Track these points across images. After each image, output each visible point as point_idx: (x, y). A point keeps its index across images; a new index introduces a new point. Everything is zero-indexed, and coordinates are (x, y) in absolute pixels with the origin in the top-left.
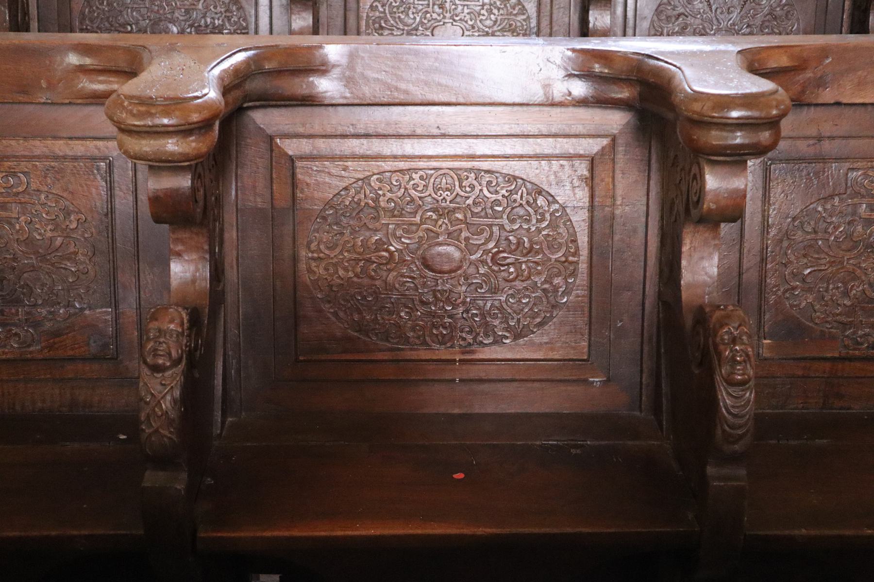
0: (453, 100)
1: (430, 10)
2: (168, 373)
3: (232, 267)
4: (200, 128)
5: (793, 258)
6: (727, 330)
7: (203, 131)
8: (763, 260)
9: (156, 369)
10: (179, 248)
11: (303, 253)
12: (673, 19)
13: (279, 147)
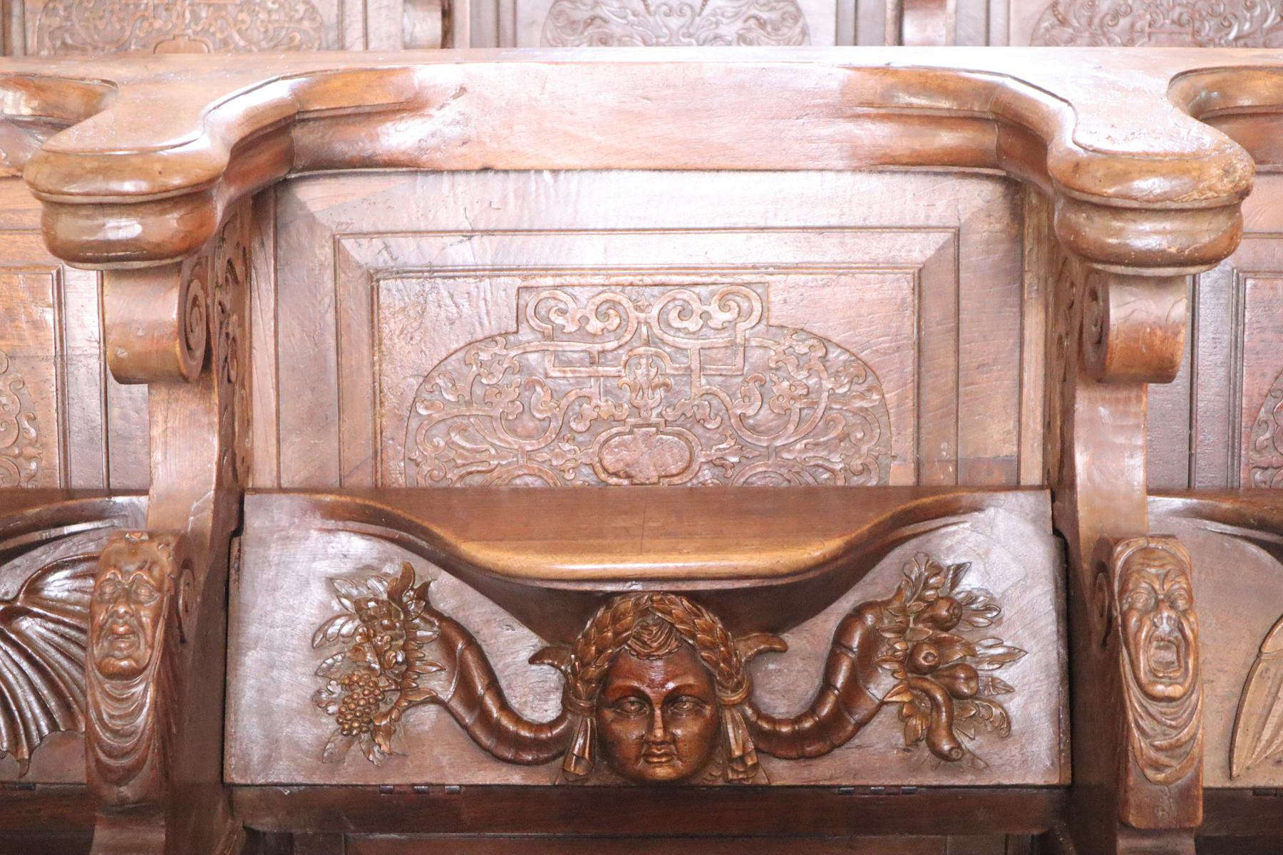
6: (112, 576)
8: (376, 452)
12: (581, 26)
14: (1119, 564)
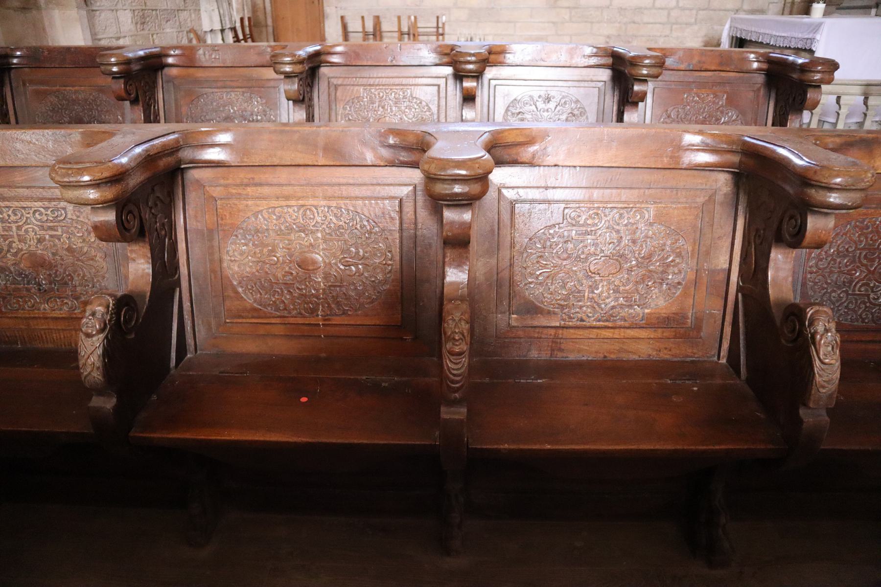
0: (310, 163)
1: (377, 109)
2: (94, 339)
3: (184, 266)
4: (106, 183)
5: (529, 264)
7: (109, 184)
9: (89, 335)
10: (134, 256)
11: (226, 258)
13: (208, 192)
14: (809, 315)
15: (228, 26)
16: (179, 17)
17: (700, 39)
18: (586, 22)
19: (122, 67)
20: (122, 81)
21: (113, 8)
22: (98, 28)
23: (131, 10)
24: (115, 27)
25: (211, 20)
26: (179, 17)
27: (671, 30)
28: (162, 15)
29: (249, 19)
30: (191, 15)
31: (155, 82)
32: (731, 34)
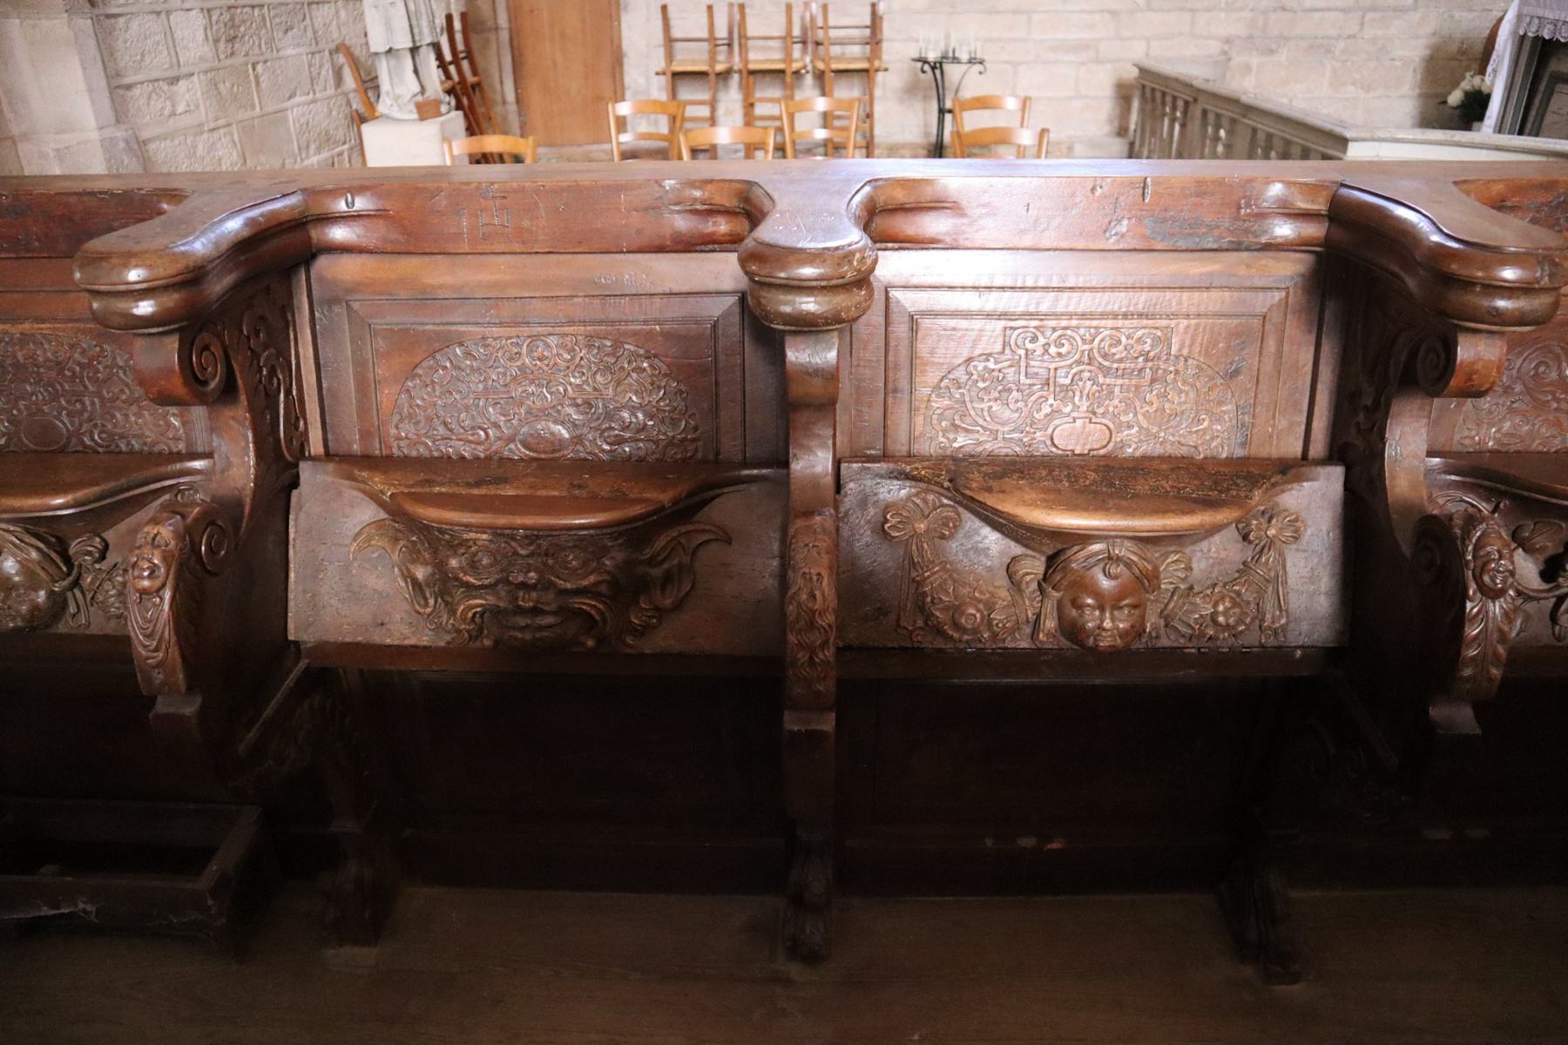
15: (428, 40)
16: (311, 19)
17: (1423, 42)
18: (1182, 9)
19: (172, 300)
20: (173, 343)
21: (159, 9)
22: (124, 59)
23: (202, 9)
24: (166, 53)
25: (388, 25)
26: (311, 19)
27: (1362, 24)
28: (276, 16)
29: (464, 16)
30: (337, 12)
31: (286, 310)
32: (1521, 33)
